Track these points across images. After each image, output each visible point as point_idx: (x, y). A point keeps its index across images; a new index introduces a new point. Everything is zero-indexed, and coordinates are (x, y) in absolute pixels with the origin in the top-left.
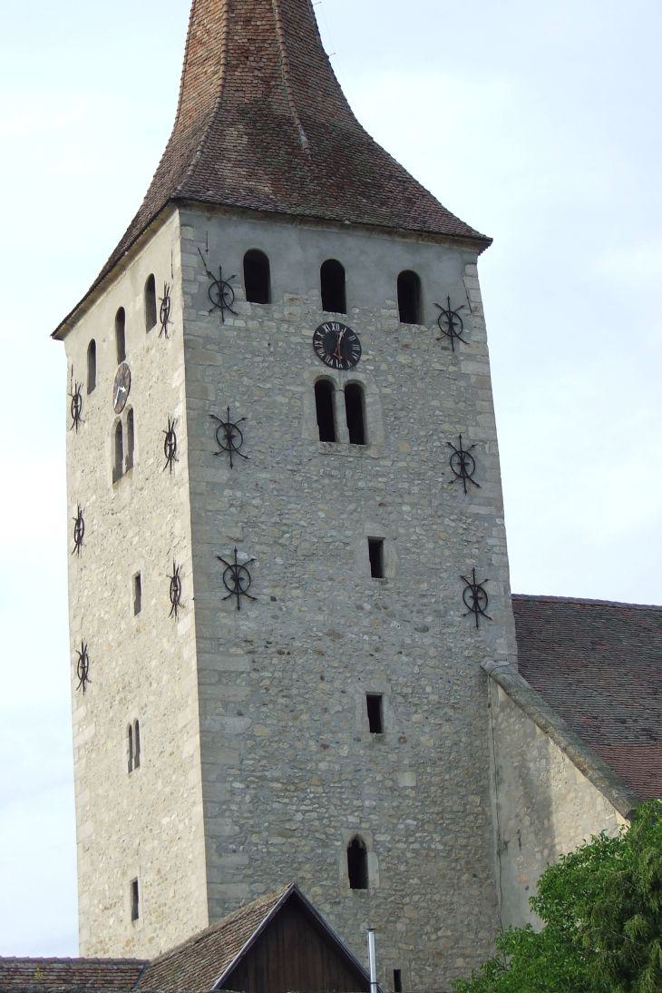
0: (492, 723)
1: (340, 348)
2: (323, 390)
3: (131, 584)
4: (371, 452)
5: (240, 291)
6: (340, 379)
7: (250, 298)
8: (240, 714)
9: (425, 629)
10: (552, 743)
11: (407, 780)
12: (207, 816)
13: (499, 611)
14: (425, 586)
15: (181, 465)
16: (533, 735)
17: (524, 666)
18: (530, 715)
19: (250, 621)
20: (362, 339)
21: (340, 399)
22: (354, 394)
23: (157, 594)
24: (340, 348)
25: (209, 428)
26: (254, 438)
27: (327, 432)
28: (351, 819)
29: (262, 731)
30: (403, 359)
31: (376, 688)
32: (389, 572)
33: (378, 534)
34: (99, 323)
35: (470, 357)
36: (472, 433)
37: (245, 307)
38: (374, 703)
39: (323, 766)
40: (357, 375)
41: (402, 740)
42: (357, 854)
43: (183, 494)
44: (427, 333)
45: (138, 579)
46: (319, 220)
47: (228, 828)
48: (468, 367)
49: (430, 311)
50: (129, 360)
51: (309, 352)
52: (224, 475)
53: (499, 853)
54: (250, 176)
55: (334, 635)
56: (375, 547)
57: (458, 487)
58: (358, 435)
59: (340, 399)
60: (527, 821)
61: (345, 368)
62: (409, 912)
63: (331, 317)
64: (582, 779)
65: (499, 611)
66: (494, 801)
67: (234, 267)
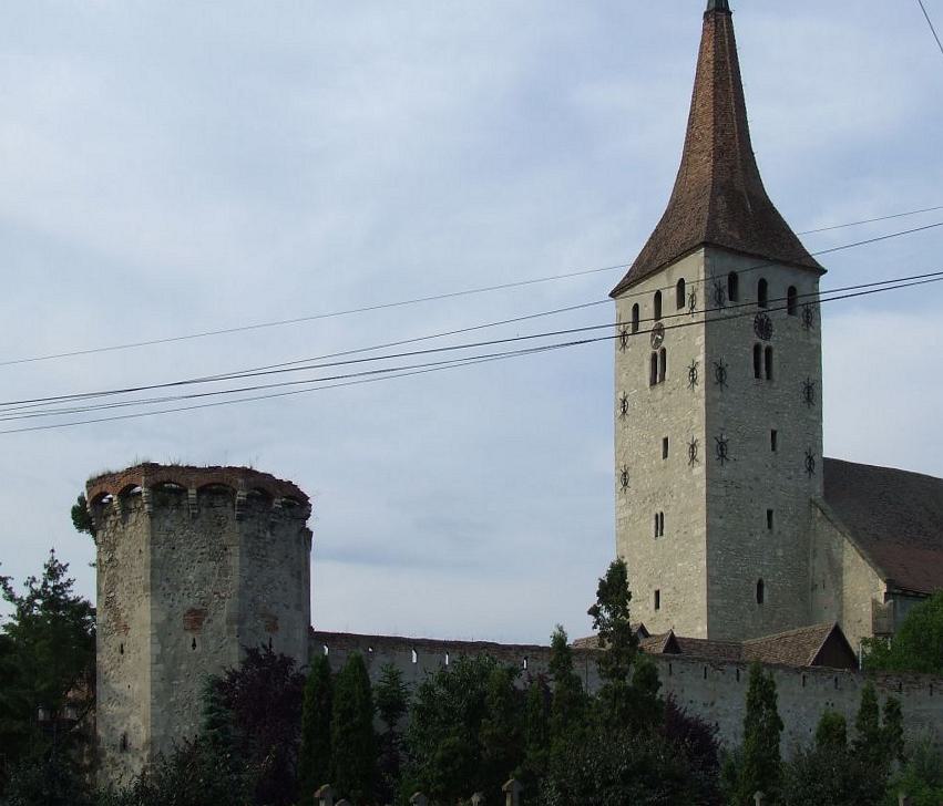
0: (813, 527)
1: (764, 328)
2: (757, 348)
4: (775, 385)
5: (727, 295)
7: (731, 299)
8: (721, 517)
9: (790, 478)
10: (846, 541)
11: (780, 553)
12: (708, 567)
13: (818, 469)
14: (791, 456)
15: (700, 387)
16: (836, 536)
17: (826, 496)
18: (836, 527)
19: (725, 471)
20: (774, 323)
21: (763, 355)
22: (769, 351)
23: (679, 451)
24: (764, 328)
25: (713, 368)
27: (757, 375)
28: (760, 571)
30: (788, 334)
31: (771, 508)
32: (778, 449)
33: (775, 429)
35: (814, 335)
36: (813, 377)
37: (728, 303)
38: (770, 513)
39: (750, 544)
40: (770, 343)
41: (779, 533)
42: (760, 585)
43: (701, 403)
44: (798, 320)
46: (760, 257)
47: (715, 573)
48: (813, 341)
49: (800, 310)
51: (752, 329)
52: (718, 395)
53: (812, 590)
54: (730, 229)
55: (757, 479)
56: (774, 433)
57: (806, 405)
58: (769, 377)
59: (763, 355)
60: (829, 576)
61: (766, 339)
62: (778, 616)
64: (861, 560)
65: (818, 469)
66: (811, 565)
67: (725, 281)
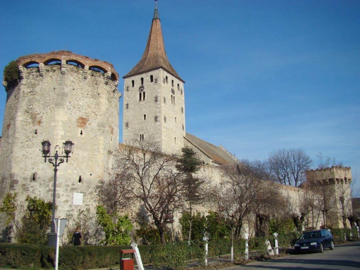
1: (173, 91)
2: (172, 96)
3: (143, 116)
4: (175, 106)
6: (173, 96)
8: (165, 137)
22: (174, 97)
24: (173, 91)
26: (166, 100)
29: (167, 140)
34: (137, 79)
40: (174, 96)
45: (145, 116)
50: (144, 84)
63: (173, 87)
67: (165, 78)
